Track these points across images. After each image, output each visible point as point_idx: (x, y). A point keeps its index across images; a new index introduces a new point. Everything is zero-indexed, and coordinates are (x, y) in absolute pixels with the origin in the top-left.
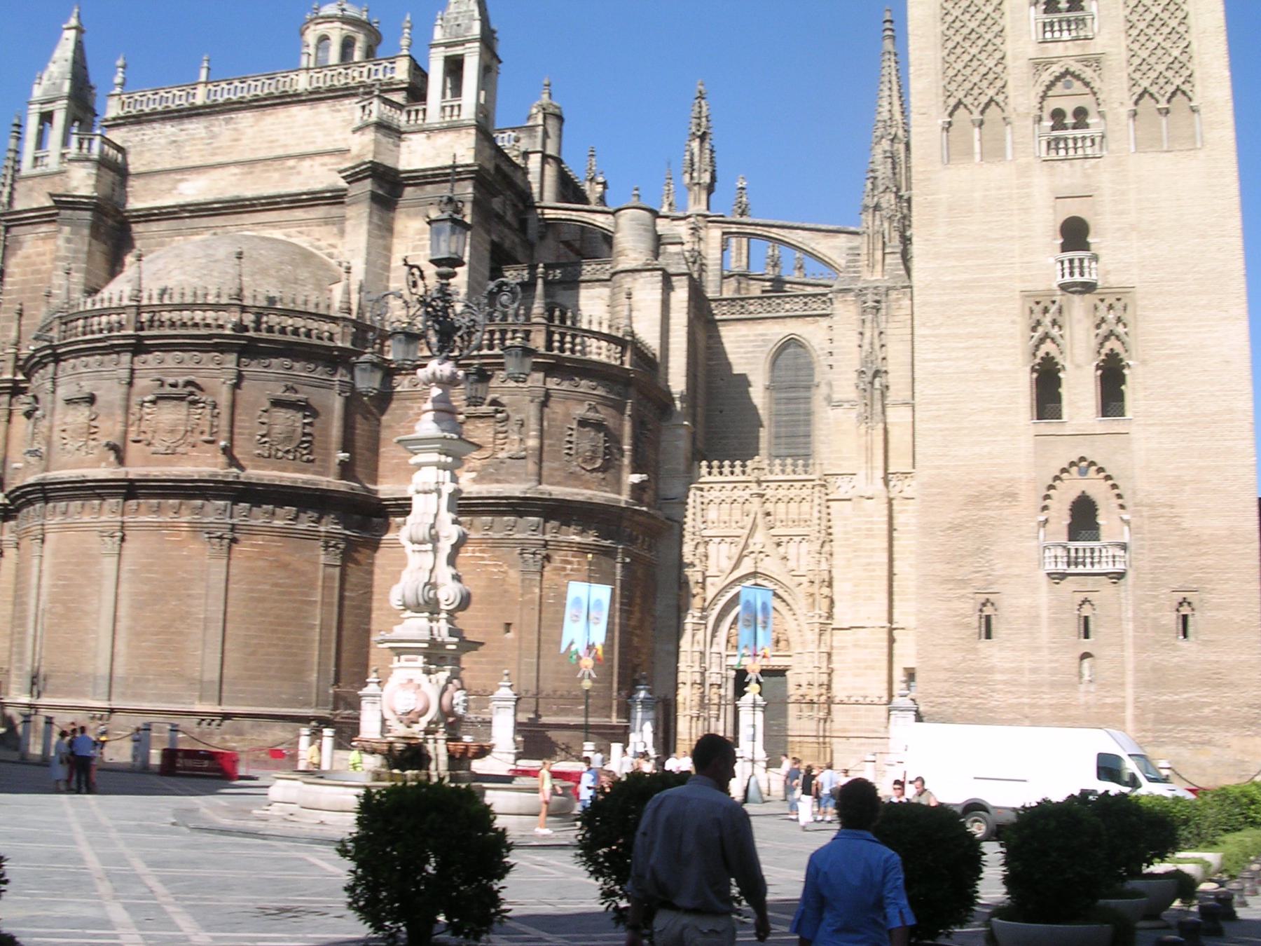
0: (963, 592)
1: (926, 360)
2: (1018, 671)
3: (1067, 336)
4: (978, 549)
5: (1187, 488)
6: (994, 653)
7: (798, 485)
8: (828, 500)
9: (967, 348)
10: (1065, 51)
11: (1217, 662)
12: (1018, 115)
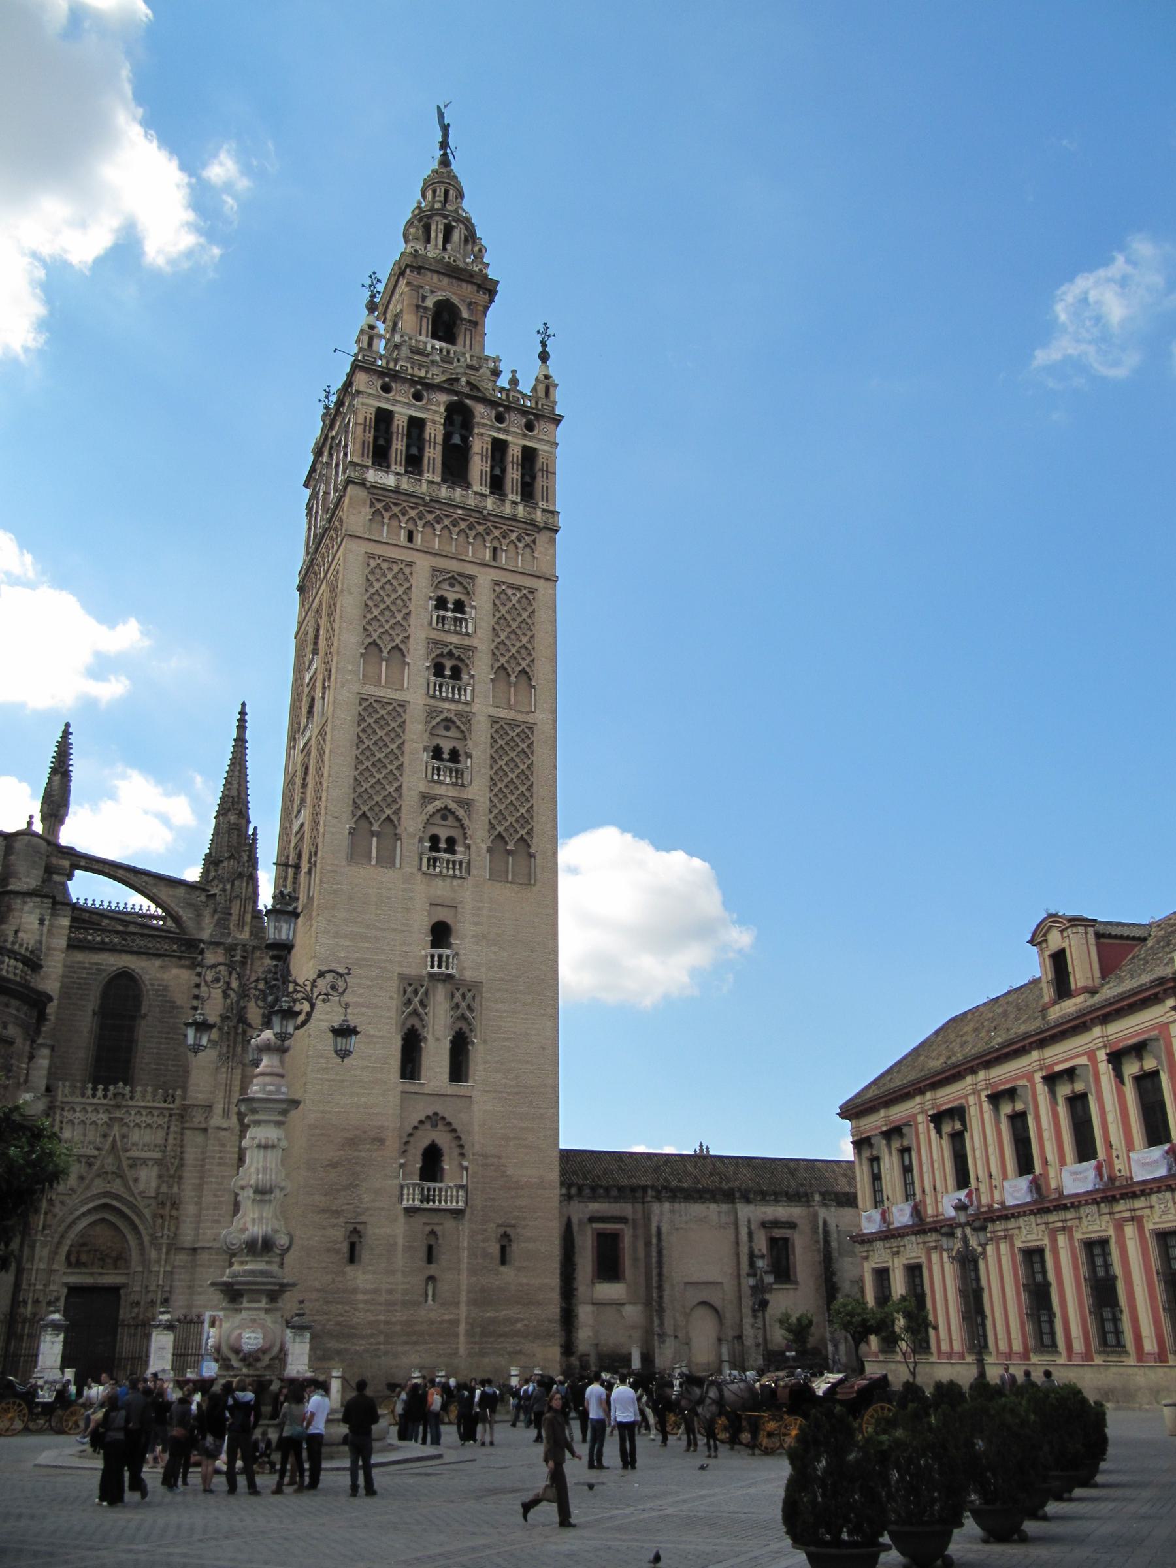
0: (336, 1221)
2: (376, 1291)
3: (431, 1014)
4: (351, 1184)
5: (511, 1143)
6: (361, 1278)
7: (156, 1113)
10: (446, 791)
11: (528, 1285)
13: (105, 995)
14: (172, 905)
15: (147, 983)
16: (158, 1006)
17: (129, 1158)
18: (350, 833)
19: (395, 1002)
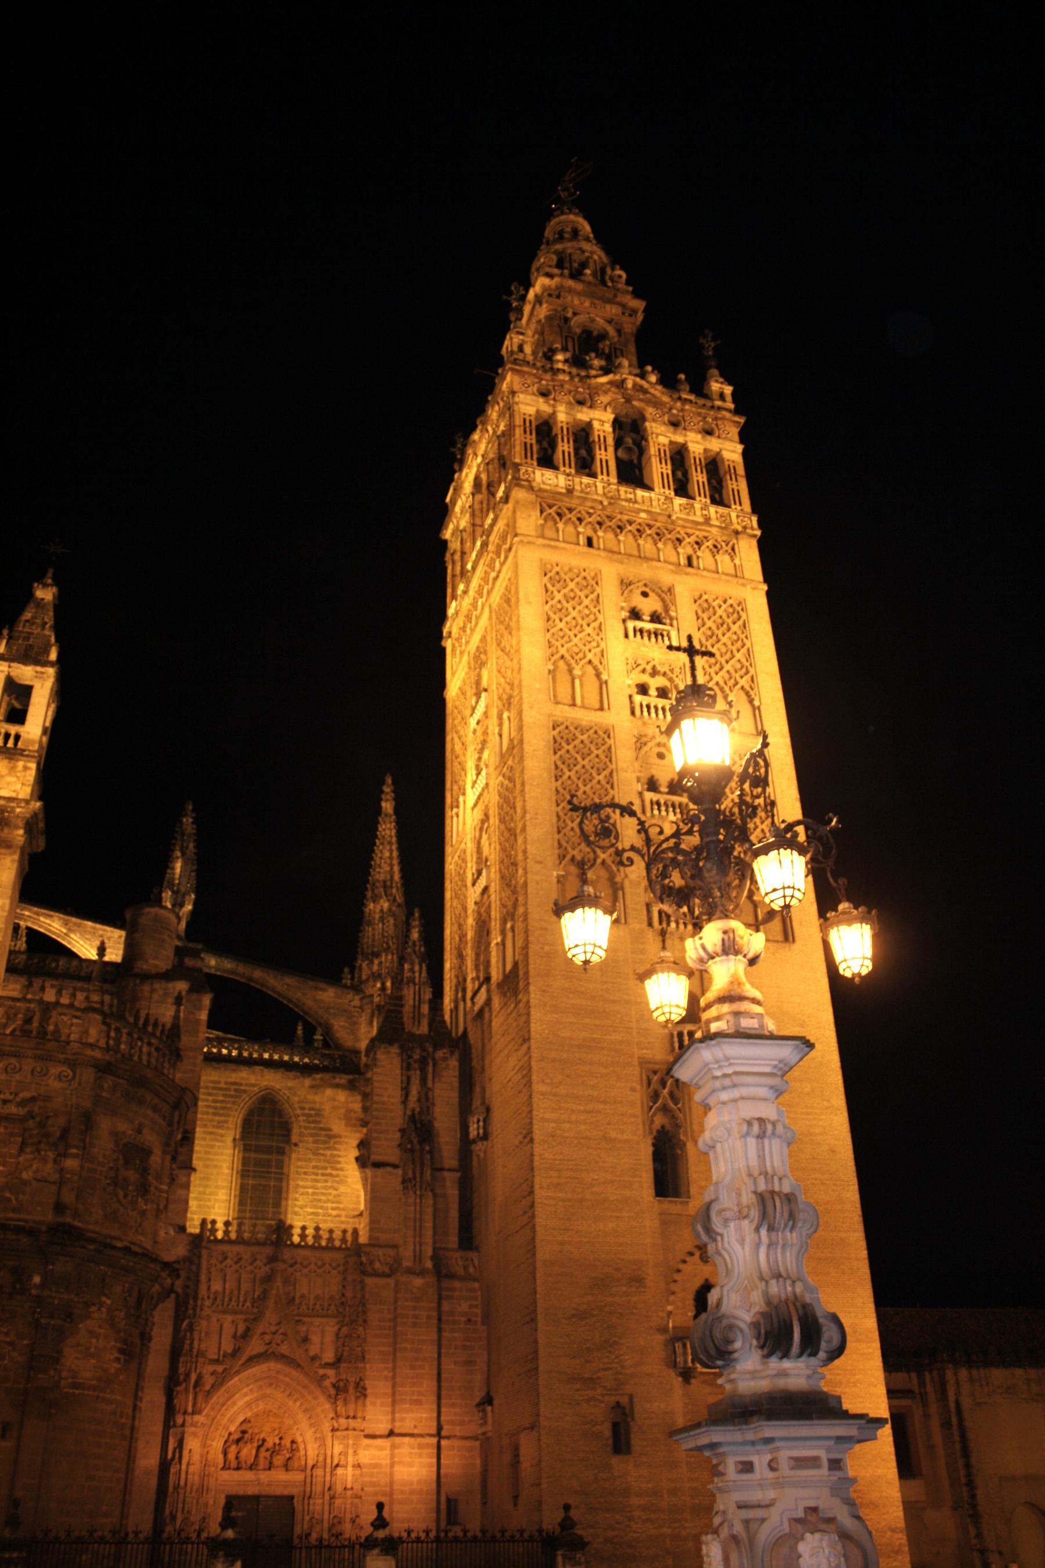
1: (544, 1120)
9: (588, 1112)
12: (631, 882)
15: (296, 1106)
18: (558, 882)
19: (638, 1095)
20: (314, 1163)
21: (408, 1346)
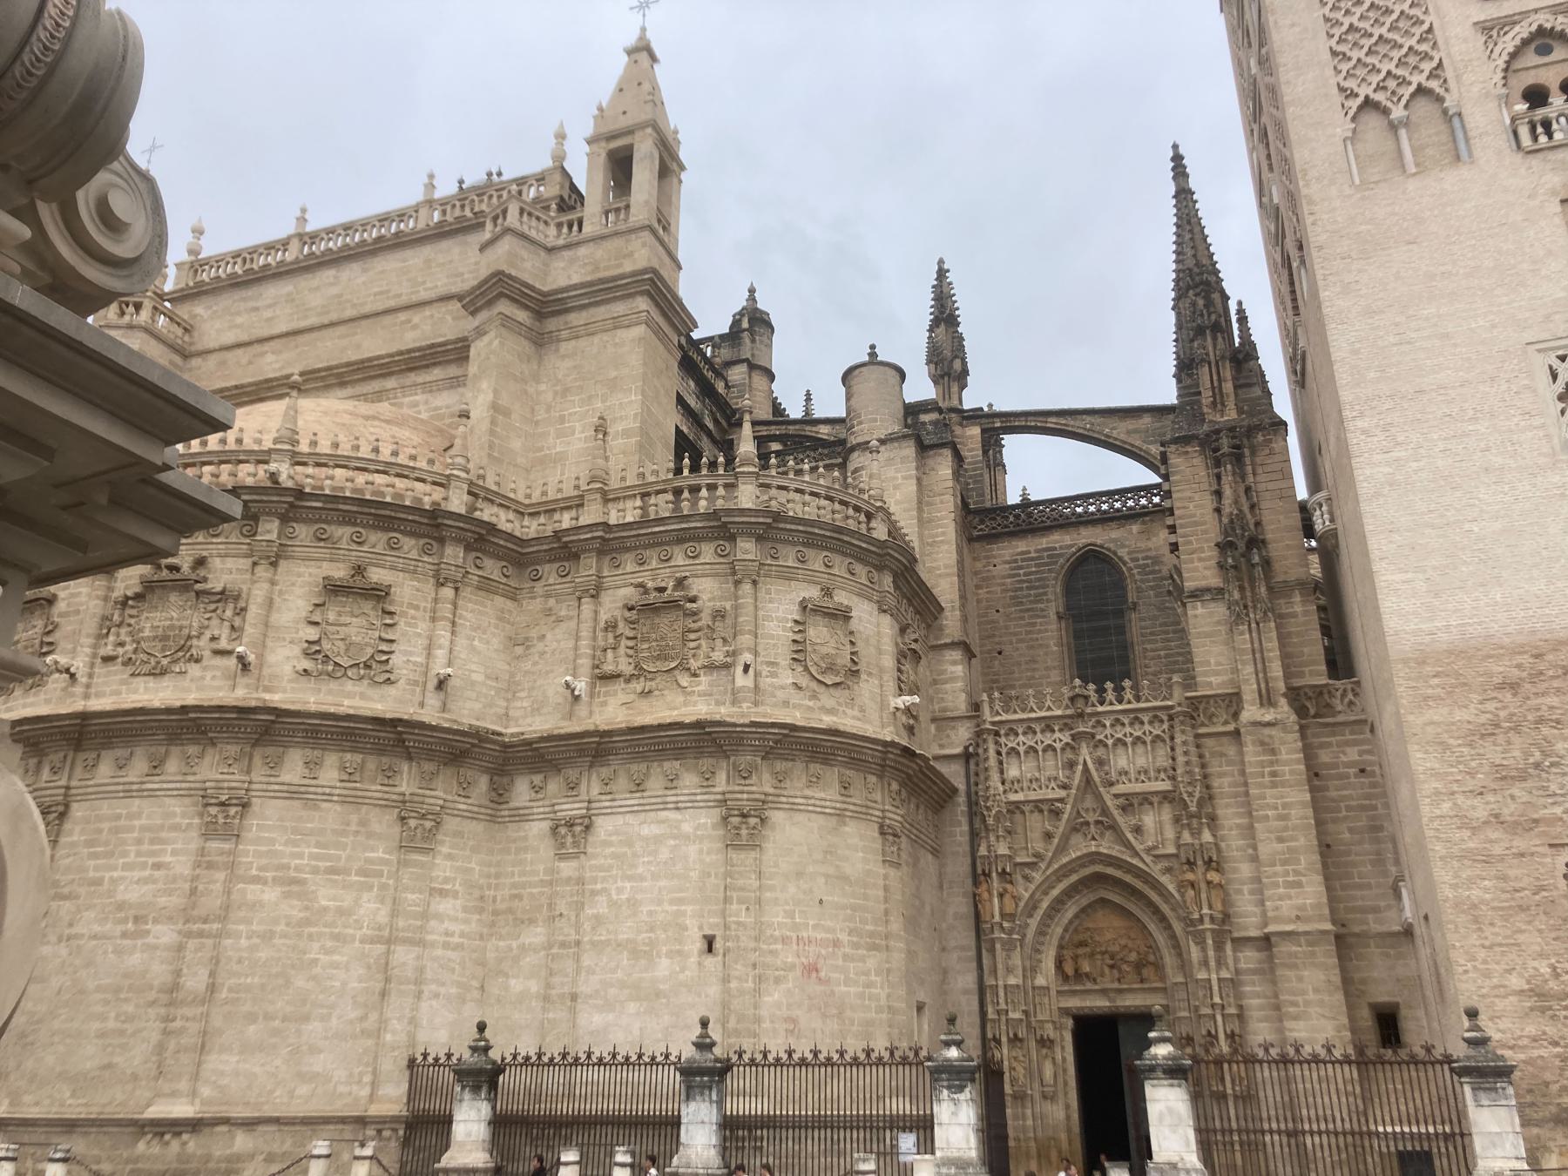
8: (1197, 736)
13: (1069, 590)
14: (1137, 443)
15: (1126, 558)
16: (1152, 588)
17: (1116, 796)
20: (1161, 620)
21: (1270, 813)
